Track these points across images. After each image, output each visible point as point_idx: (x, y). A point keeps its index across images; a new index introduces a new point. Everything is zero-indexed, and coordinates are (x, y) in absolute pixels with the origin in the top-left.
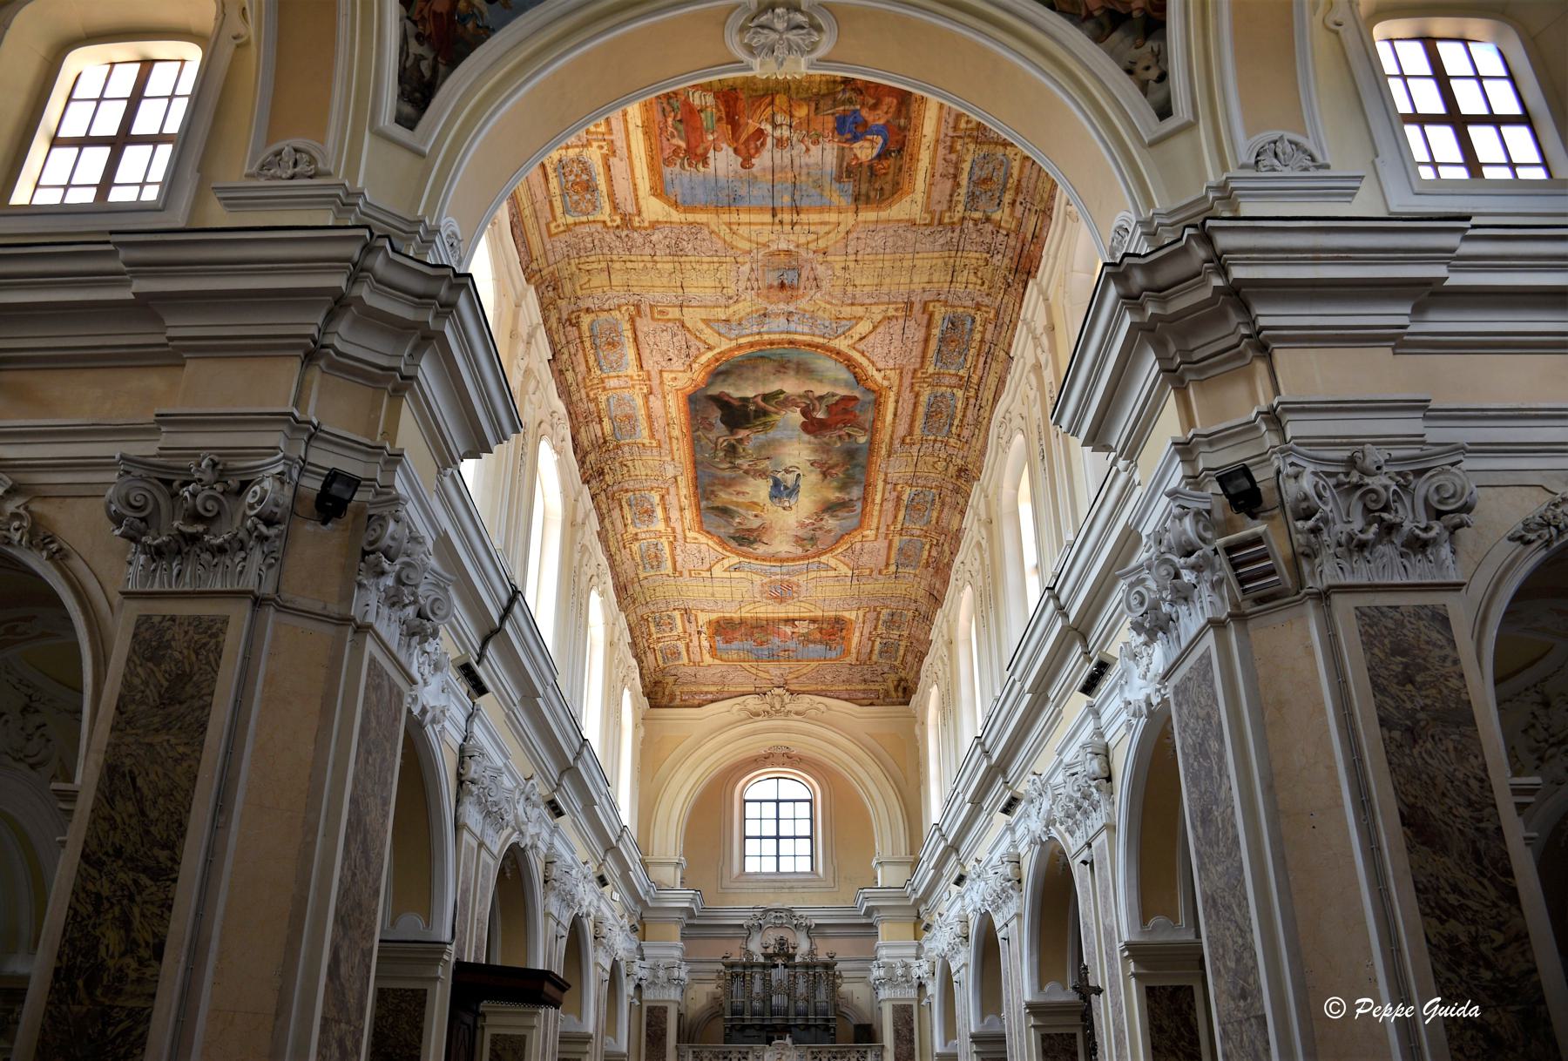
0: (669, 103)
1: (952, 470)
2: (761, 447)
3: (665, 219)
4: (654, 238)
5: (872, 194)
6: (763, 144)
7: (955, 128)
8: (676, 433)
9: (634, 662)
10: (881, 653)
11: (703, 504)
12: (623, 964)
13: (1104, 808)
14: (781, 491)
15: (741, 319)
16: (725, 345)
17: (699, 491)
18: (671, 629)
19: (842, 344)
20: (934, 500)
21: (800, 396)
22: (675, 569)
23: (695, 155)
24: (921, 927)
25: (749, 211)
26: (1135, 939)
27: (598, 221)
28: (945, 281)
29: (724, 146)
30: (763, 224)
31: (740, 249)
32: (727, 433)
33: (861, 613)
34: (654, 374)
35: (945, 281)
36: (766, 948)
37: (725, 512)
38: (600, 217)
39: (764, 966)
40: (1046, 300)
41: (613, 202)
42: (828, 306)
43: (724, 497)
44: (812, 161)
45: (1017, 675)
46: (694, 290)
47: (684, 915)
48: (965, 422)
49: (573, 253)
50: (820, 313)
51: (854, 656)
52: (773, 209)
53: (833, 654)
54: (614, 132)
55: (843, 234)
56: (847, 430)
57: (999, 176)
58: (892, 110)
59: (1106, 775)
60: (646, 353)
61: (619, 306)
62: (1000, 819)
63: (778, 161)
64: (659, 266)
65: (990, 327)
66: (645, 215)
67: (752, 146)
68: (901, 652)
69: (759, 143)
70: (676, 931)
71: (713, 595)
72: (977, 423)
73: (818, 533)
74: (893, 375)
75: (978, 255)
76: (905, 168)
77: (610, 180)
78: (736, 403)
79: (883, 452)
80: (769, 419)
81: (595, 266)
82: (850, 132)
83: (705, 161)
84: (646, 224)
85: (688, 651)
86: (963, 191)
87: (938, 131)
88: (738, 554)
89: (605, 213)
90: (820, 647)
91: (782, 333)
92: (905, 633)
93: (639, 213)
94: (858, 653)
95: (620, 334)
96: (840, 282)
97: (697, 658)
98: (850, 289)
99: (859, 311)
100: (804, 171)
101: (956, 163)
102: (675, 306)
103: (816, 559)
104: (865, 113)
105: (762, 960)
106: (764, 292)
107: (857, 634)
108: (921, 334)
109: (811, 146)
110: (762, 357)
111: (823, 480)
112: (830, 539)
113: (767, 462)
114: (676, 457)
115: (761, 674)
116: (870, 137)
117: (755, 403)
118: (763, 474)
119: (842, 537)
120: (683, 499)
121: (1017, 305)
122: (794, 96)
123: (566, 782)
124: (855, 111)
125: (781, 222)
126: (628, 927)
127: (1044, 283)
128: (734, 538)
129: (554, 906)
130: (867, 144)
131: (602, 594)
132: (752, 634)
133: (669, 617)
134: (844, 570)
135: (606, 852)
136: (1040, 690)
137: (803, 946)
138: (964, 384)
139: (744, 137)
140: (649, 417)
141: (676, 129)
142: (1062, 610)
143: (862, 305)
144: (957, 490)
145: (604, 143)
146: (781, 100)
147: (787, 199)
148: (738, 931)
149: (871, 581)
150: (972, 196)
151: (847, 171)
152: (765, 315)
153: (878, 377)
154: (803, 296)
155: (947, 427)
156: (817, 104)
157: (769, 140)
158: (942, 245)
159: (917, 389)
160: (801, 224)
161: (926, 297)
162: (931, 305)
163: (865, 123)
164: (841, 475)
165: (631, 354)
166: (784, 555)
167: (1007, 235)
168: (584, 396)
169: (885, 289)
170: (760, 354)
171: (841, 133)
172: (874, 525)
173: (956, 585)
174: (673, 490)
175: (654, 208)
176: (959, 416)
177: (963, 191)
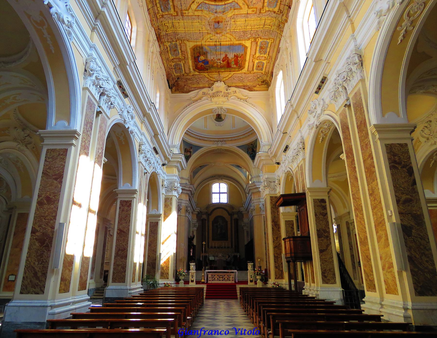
4: (250, 36)
5: (199, 49)
7: (185, 61)
23: (236, 57)
25: (226, 45)
27: (262, 39)
29: (230, 59)
30: (223, 41)
31: (229, 34)
44: (213, 56)
52: (221, 45)
55: (204, 39)
63: (220, 56)
66: (251, 42)
75: (169, 32)
76: (193, 54)
77: (256, 50)
84: (251, 39)
86: (179, 48)
104: (203, 65)
109: (213, 59)
125: (219, 42)
130: (202, 59)
141: (239, 61)
147: (218, 47)
151: (205, 54)
157: (221, 60)
158: (179, 34)
163: (203, 63)
175: (248, 44)
177: (179, 48)
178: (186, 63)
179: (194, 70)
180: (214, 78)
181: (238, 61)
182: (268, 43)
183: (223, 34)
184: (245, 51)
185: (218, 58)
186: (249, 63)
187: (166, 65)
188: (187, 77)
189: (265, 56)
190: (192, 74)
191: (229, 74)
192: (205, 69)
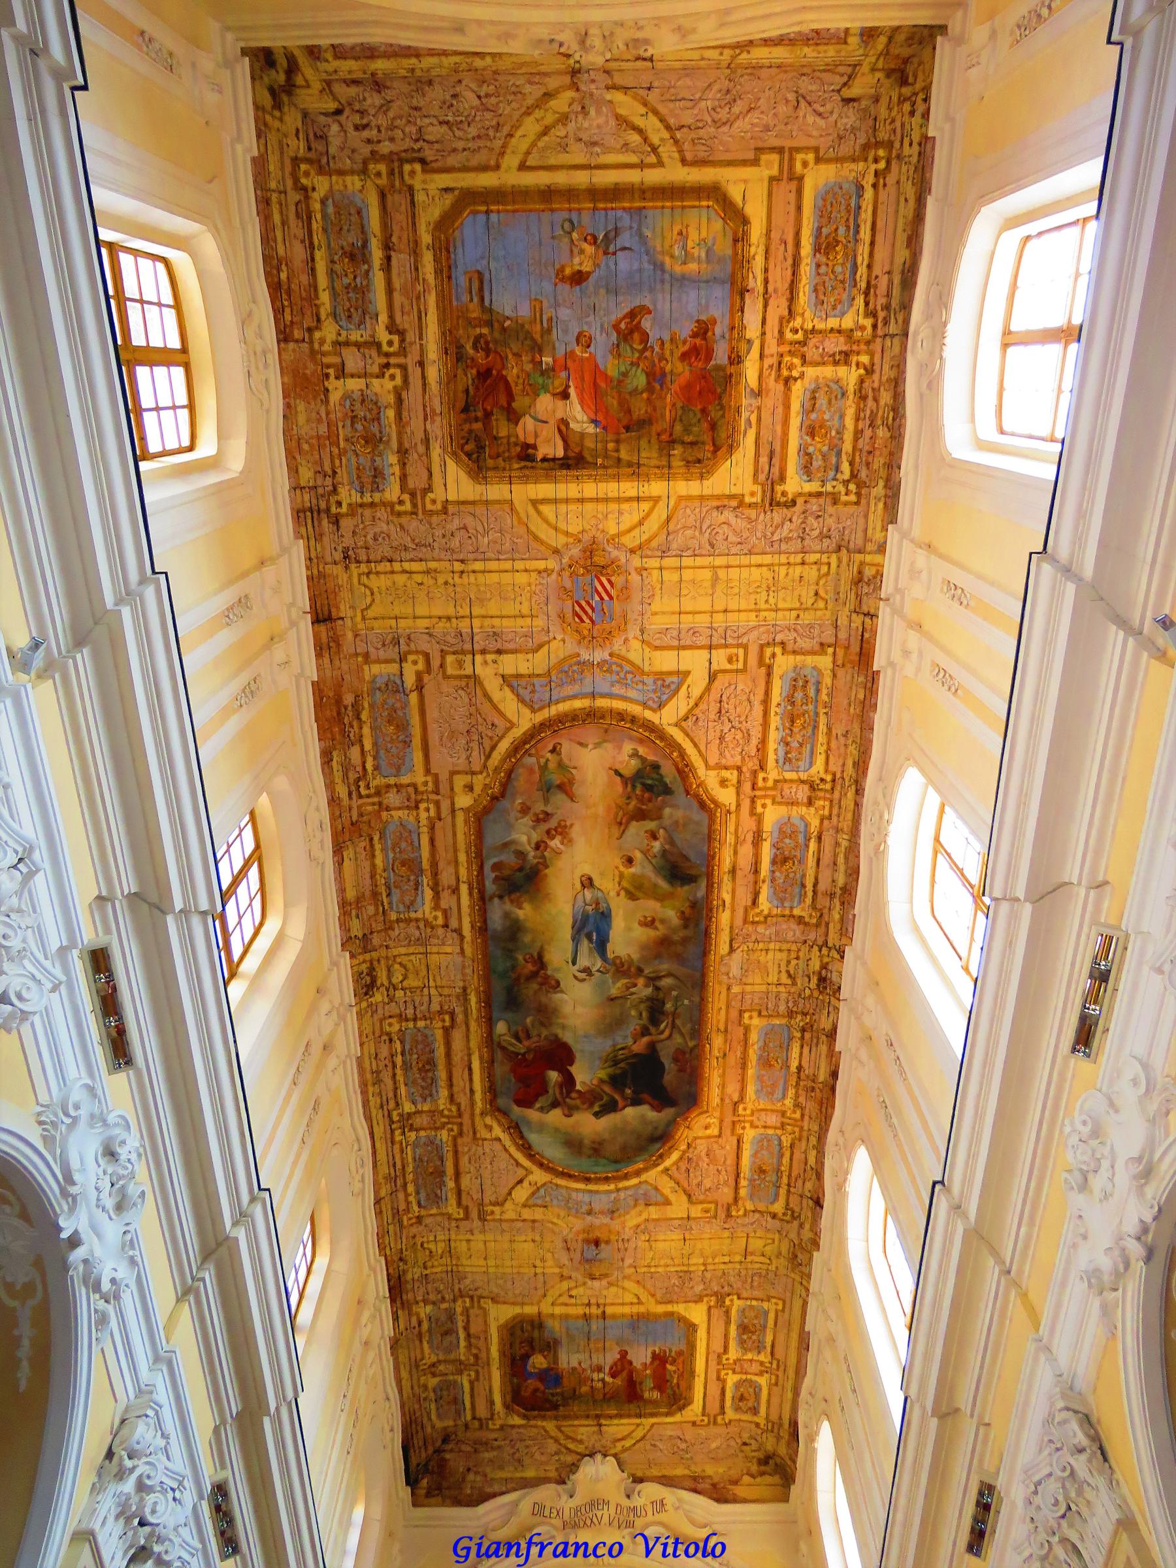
1: (382, 977)
4: (701, 1287)
5: (529, 1328)
6: (611, 1368)
7: (477, 1372)
8: (718, 1041)
15: (635, 1205)
16: (651, 1175)
17: (702, 926)
19: (539, 1176)
21: (577, 1108)
23: (660, 1360)
25: (623, 1315)
28: (455, 1241)
30: (612, 1304)
32: (659, 1046)
34: (727, 1131)
35: (455, 1241)
38: (741, 1302)
42: (555, 1220)
46: (674, 1237)
48: (390, 1068)
49: (771, 1275)
50: (562, 1214)
55: (550, 1293)
56: (521, 1048)
57: (437, 1339)
60: (731, 1161)
61: (745, 1215)
63: (601, 1356)
64: (701, 1261)
65: (402, 1206)
73: (539, 807)
74: (483, 1133)
75: (435, 1270)
76: (507, 1347)
78: (645, 1096)
80: (610, 1070)
83: (655, 1356)
84: (705, 1299)
86: (460, 1324)
89: (736, 1305)
91: (597, 1192)
93: (710, 1308)
95: (752, 1181)
96: (547, 1245)
98: (538, 1238)
99: (527, 1214)
100: (581, 1348)
102: (695, 1218)
104: (542, 1388)
106: (613, 1238)
108: (465, 1182)
110: (616, 1162)
111: (542, 948)
113: (614, 992)
117: (624, 1098)
118: (621, 969)
125: (598, 1305)
138: (406, 1123)
139: (624, 1374)
140: (744, 1066)
143: (524, 1220)
146: (600, 1396)
147: (594, 1327)
151: (551, 1347)
152: (613, 1212)
153: (498, 1131)
154: (578, 1233)
155: (407, 1047)
157: (607, 1370)
159: (454, 1108)
160: (583, 1305)
162: (462, 1216)
164: (520, 958)
166: (590, 733)
169: (507, 1237)
170: (618, 1166)
172: (460, 818)
174: (739, 922)
175: (697, 1314)
176: (399, 1072)
177: (460, 1324)
178: (481, 1378)
179: (506, 1406)
180: (581, 1442)
181: (668, 1377)
182: (766, 1313)
183: (612, 1279)
184: (688, 1337)
185: (595, 1361)
187: (406, 1384)
188: (478, 1434)
189: (762, 1357)
190: (498, 1423)
191: (633, 1427)
192: (548, 1406)
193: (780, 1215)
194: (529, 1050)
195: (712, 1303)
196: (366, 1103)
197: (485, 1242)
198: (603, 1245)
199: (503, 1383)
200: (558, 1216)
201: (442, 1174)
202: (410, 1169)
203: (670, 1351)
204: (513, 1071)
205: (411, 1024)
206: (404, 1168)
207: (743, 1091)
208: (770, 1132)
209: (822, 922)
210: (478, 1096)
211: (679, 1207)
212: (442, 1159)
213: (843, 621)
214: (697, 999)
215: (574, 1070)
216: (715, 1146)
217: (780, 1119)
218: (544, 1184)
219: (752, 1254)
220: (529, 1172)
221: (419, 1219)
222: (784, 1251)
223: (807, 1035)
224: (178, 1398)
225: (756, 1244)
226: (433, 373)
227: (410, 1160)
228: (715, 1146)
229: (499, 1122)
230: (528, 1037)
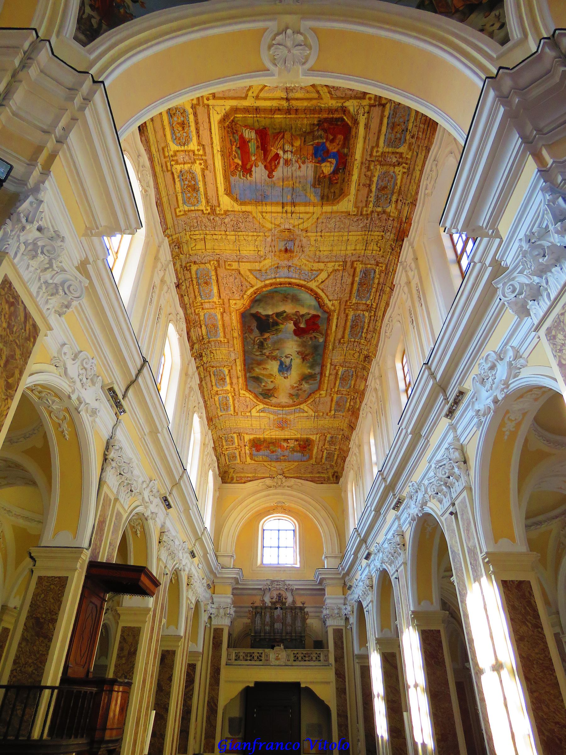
0: (233, 137)
1: (362, 357)
2: (274, 343)
3: (231, 209)
4: (226, 221)
6: (278, 163)
7: (371, 155)
8: (236, 335)
9: (215, 458)
10: (326, 458)
11: (248, 375)
12: (202, 604)
13: (463, 479)
14: (284, 368)
15: (266, 270)
16: (259, 284)
17: (246, 367)
18: (233, 444)
19: (313, 285)
20: (353, 375)
21: (293, 314)
22: (235, 411)
23: (247, 170)
24: (346, 587)
25: (272, 204)
26: (490, 550)
27: (199, 210)
28: (362, 250)
29: (260, 164)
30: (278, 213)
32: (259, 335)
33: (318, 436)
34: (226, 301)
35: (362, 250)
36: (272, 599)
37: (257, 379)
38: (201, 208)
39: (271, 608)
40: (413, 247)
41: (207, 198)
42: (307, 263)
43: (257, 371)
45: (403, 426)
46: (245, 252)
47: (233, 581)
48: (369, 330)
49: (188, 229)
50: (303, 267)
51: (314, 459)
52: (283, 203)
53: (305, 458)
54: (207, 154)
55: (315, 220)
56: (314, 334)
57: (390, 186)
58: (341, 143)
59: (463, 460)
61: (210, 261)
62: (392, 514)
63: (285, 174)
64: (229, 237)
65: (383, 275)
66: (222, 206)
67: (273, 164)
68: (336, 458)
69: (276, 162)
70: (229, 590)
71: (251, 425)
72: (375, 330)
73: (300, 392)
74: (336, 303)
77: (205, 184)
78: (264, 318)
79: (331, 347)
80: (278, 327)
81: (198, 237)
82: (321, 156)
83: (249, 171)
84: (222, 212)
85: (240, 456)
86: (373, 195)
87: (362, 157)
88: (263, 403)
89: (202, 206)
90: (300, 454)
91: (285, 278)
92: (337, 447)
93: (219, 206)
94: (316, 458)
96: (313, 249)
97: (244, 460)
98: (318, 253)
99: (321, 266)
101: (370, 178)
102: (236, 262)
103: (298, 407)
104: (328, 144)
105: (270, 605)
106: (277, 253)
107: (316, 448)
108: (350, 281)
109: (302, 165)
110: (276, 292)
111: (303, 363)
112: (305, 395)
113: (277, 351)
114: (236, 349)
115: (272, 468)
116: (329, 160)
117: (273, 318)
118: (275, 358)
119: (310, 394)
120: (238, 372)
121: (397, 260)
122: (294, 133)
123: (175, 492)
124: (324, 143)
125: (286, 212)
126: (205, 585)
127: (412, 240)
128: (261, 394)
129: (164, 555)
130: (328, 164)
131: (200, 417)
132: (269, 447)
133: (232, 437)
134: (311, 413)
135: (196, 540)
136: (416, 432)
137: (290, 600)
138: (369, 308)
139: (269, 158)
140: (223, 325)
141: (237, 153)
142: (432, 375)
143: (323, 262)
144: (364, 368)
145: (202, 162)
146: (287, 136)
147: (289, 197)
148: (259, 592)
149: (323, 419)
150: (378, 198)
152: (278, 267)
153: (329, 304)
154: (296, 256)
155: (360, 334)
156: (305, 138)
157: (281, 160)
158: (362, 227)
159: (347, 312)
160: (296, 213)
161: (354, 259)
162: (355, 263)
163: (328, 151)
164: (311, 360)
165: (215, 290)
166: (284, 404)
167: (393, 220)
168: (193, 312)
169: (334, 253)
170: (275, 290)
171: (316, 157)
172: (325, 389)
173: (363, 417)
174: (234, 367)
175: (226, 202)
176: (366, 327)
177: (373, 195)
178: (369, 150)
179: (356, 122)
181: (239, 152)
182: (184, 203)
183: (278, 229)
184: (230, 186)
186: (212, 144)
187: (421, 156)
189: (179, 167)
191: (261, 95)
193: (192, 265)
194: (311, 334)
195: (218, 209)
196: (378, 342)
197: (346, 250)
198: (283, 249)
199: (355, 147)
200: (306, 265)
201: (360, 284)
202: (374, 290)
203: (240, 175)
204: (319, 327)
205: (356, 340)
206: (376, 291)
207: (222, 317)
208: (206, 301)
209: (205, 370)
210: (335, 317)
211: (245, 267)
212: (358, 290)
213: (218, 421)
214: (246, 348)
215: (294, 328)
216: (230, 295)
217: (204, 306)
218: (312, 280)
219: (201, 240)
220: (318, 287)
221: (377, 264)
222: (185, 247)
223: (201, 338)
224: (390, 529)
225: (200, 246)
226: (316, 448)
227: (372, 294)
228: (230, 295)
229: (328, 308)
230: (311, 338)
